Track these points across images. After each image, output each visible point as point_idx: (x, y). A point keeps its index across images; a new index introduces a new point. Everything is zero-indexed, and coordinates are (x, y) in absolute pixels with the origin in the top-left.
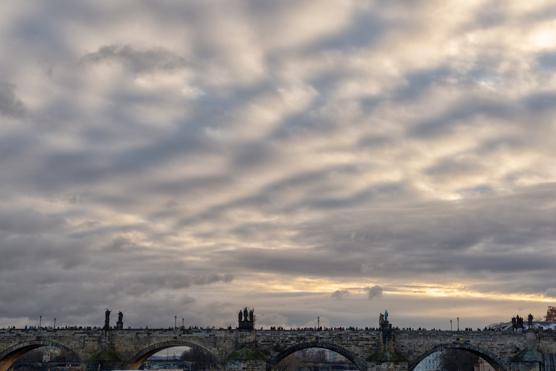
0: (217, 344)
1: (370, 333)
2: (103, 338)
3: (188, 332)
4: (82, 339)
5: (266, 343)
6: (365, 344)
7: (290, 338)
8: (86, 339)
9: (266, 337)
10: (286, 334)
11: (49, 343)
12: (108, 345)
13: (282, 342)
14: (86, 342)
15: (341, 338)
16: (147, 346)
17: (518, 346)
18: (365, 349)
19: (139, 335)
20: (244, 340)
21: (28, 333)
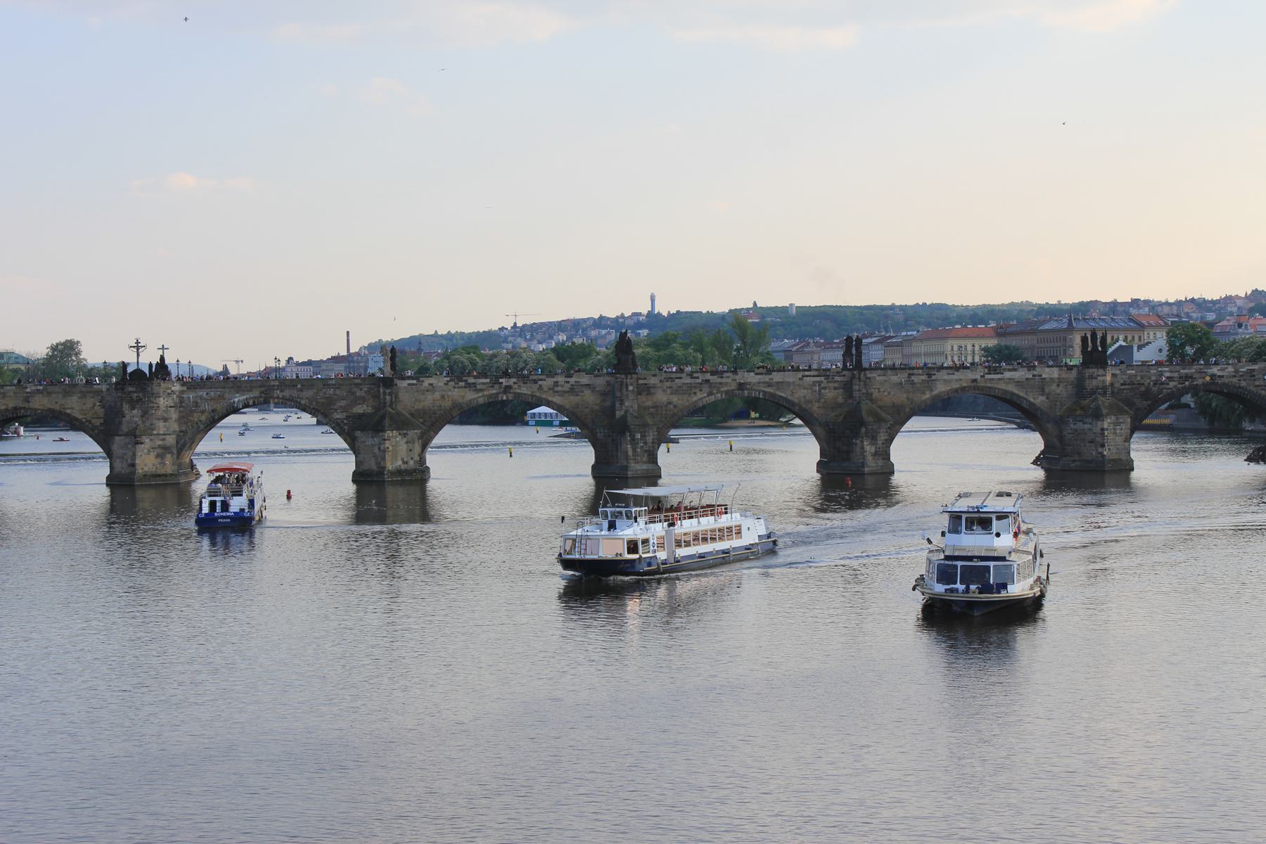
0: (1047, 391)
2: (855, 384)
5: (1127, 387)
7: (1168, 378)
8: (822, 385)
10: (1161, 371)
12: (865, 395)
13: (1155, 384)
14: (823, 391)
15: (1254, 376)
16: (927, 396)
20: (1094, 383)
21: (722, 377)
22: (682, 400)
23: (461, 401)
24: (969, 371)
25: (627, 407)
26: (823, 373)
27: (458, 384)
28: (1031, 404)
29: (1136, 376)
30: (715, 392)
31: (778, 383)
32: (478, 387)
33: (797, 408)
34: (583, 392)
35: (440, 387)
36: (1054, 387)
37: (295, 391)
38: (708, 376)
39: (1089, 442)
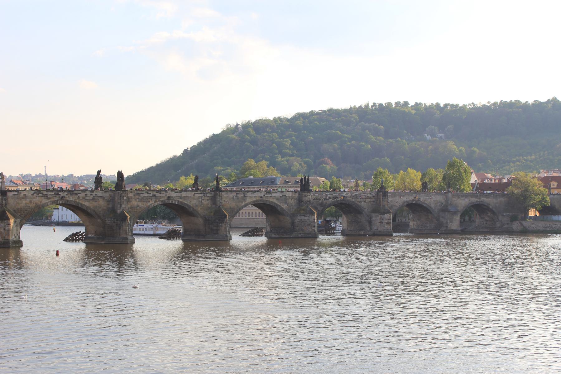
0: (287, 202)
1: (372, 194)
2: (218, 198)
3: (269, 193)
4: (199, 198)
6: (369, 201)
7: (329, 197)
8: (203, 198)
9: (315, 196)
11: (176, 201)
13: (325, 200)
15: (357, 197)
16: (244, 204)
17: (442, 202)
19: (238, 196)
21: (161, 194)
22: (144, 205)
23: (40, 204)
24: (259, 192)
25: (123, 208)
27: (38, 195)
28: (282, 208)
29: (318, 196)
30: (158, 201)
31: (184, 197)
32: (49, 196)
33: (191, 209)
35: (29, 196)
36: (290, 200)
38: (155, 193)
39: (308, 225)
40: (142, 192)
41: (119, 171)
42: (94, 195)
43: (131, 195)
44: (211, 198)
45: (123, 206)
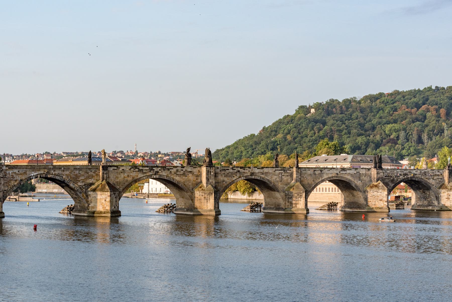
0: (361, 178)
5: (387, 178)
6: (437, 178)
7: (400, 174)
8: (283, 174)
11: (258, 177)
13: (396, 177)
14: (283, 177)
15: (426, 174)
16: (320, 180)
18: (437, 181)
21: (244, 170)
25: (210, 182)
26: (283, 169)
28: (356, 185)
29: (390, 173)
31: (266, 173)
32: (144, 171)
34: (188, 175)
36: (363, 177)
37: (61, 171)
38: (239, 169)
39: (380, 200)
40: (227, 168)
41: (207, 148)
42: (185, 171)
43: (218, 171)
44: (291, 174)
45: (210, 181)
